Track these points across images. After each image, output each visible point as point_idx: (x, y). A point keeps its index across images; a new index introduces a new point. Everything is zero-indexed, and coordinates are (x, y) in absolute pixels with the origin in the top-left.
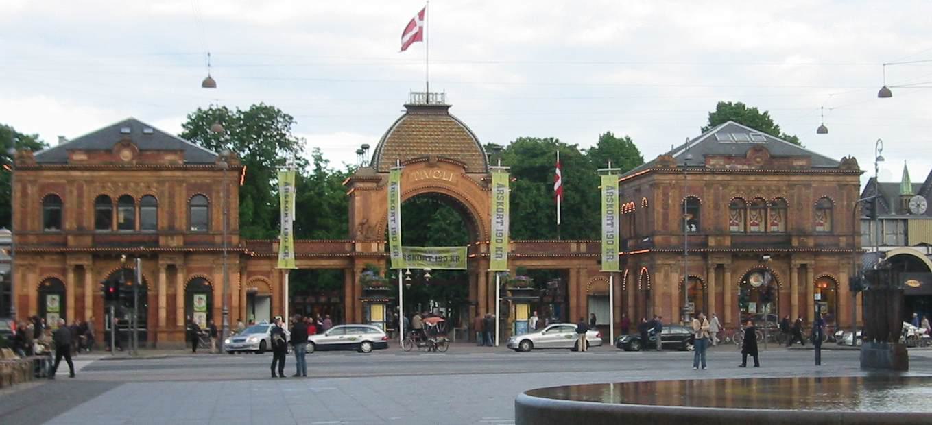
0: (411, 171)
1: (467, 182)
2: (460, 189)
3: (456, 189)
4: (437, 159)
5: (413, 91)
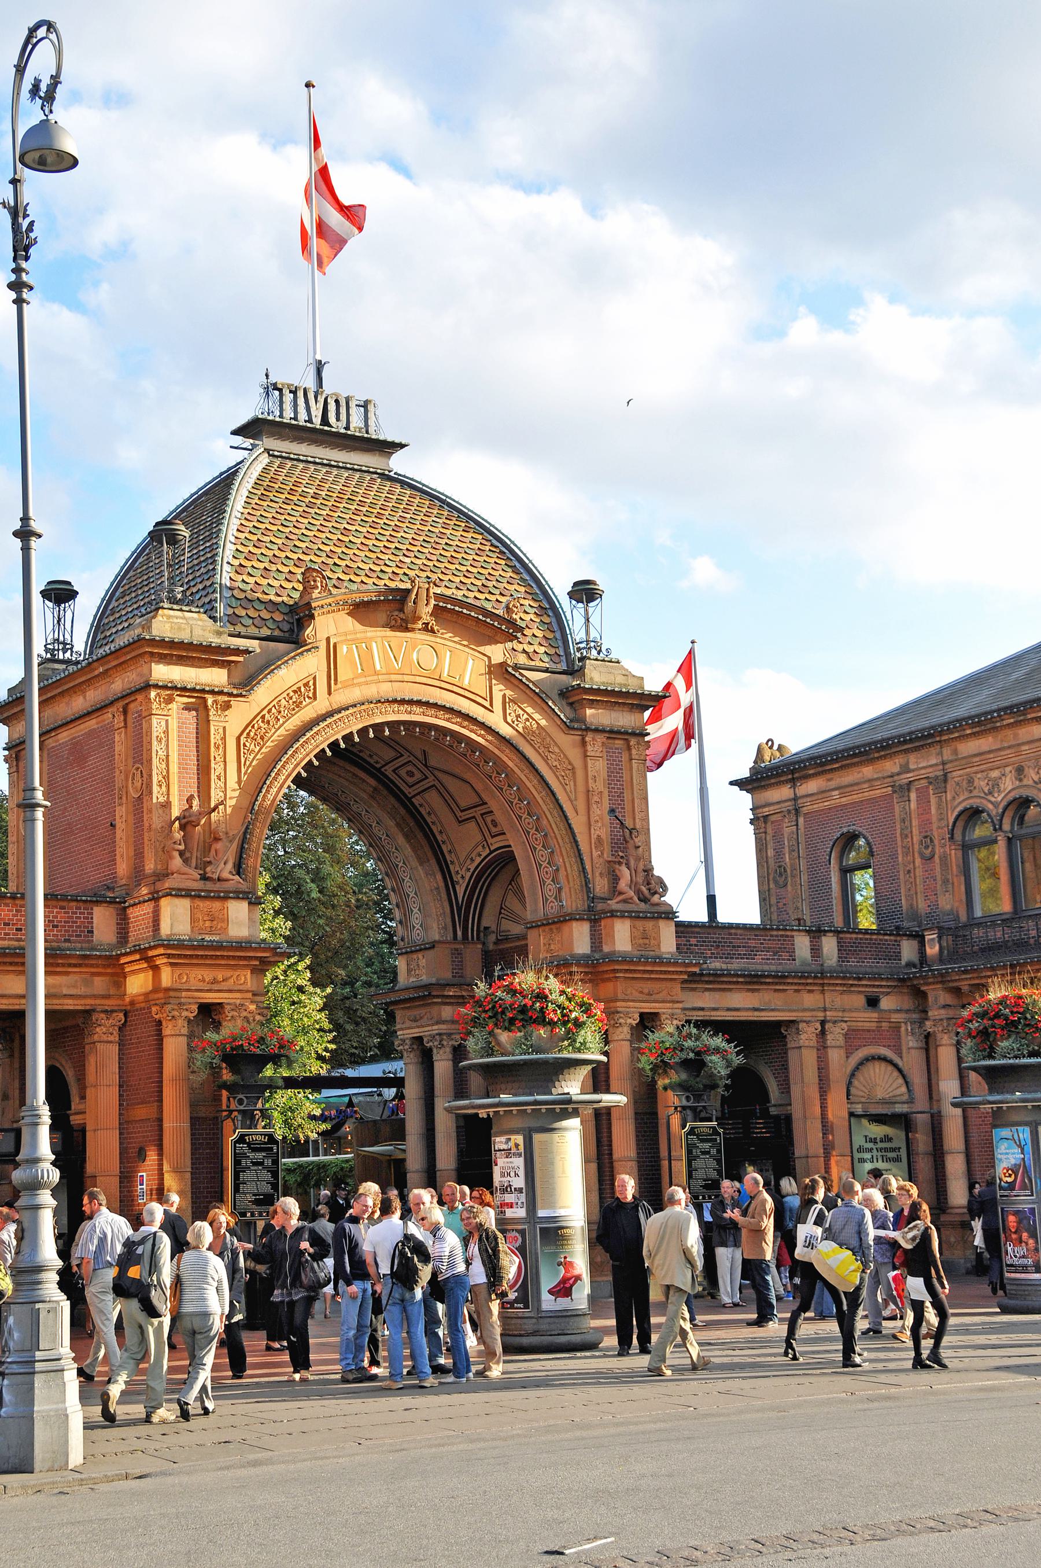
4: (433, 602)
5: (273, 379)
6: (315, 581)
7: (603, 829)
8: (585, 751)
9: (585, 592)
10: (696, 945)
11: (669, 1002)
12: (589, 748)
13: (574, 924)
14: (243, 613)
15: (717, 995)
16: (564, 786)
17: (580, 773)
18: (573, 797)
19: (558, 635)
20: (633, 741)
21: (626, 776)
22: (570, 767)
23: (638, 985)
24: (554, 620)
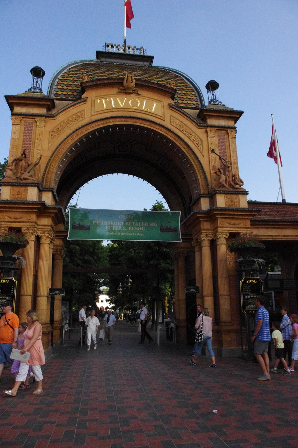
0: (101, 97)
1: (177, 115)
2: (167, 123)
3: (163, 123)
6: (85, 77)
7: (217, 163)
8: (208, 134)
9: (212, 86)
10: (268, 211)
11: (244, 228)
12: (209, 133)
13: (202, 199)
14: (61, 93)
15: (279, 231)
16: (197, 147)
17: (205, 143)
18: (201, 151)
19: (198, 98)
20: (229, 131)
21: (227, 143)
22: (200, 140)
23: (229, 221)
24: (196, 93)
